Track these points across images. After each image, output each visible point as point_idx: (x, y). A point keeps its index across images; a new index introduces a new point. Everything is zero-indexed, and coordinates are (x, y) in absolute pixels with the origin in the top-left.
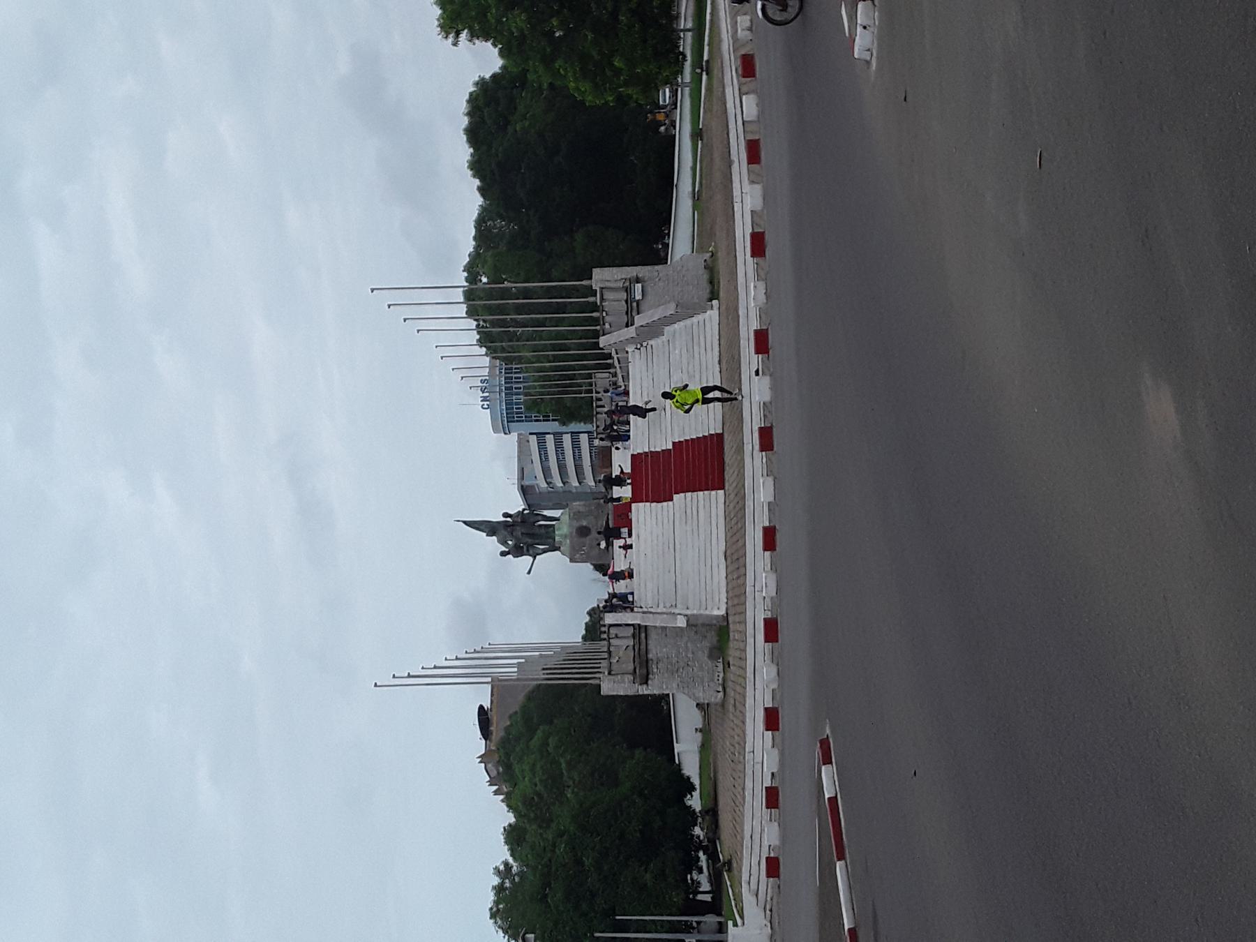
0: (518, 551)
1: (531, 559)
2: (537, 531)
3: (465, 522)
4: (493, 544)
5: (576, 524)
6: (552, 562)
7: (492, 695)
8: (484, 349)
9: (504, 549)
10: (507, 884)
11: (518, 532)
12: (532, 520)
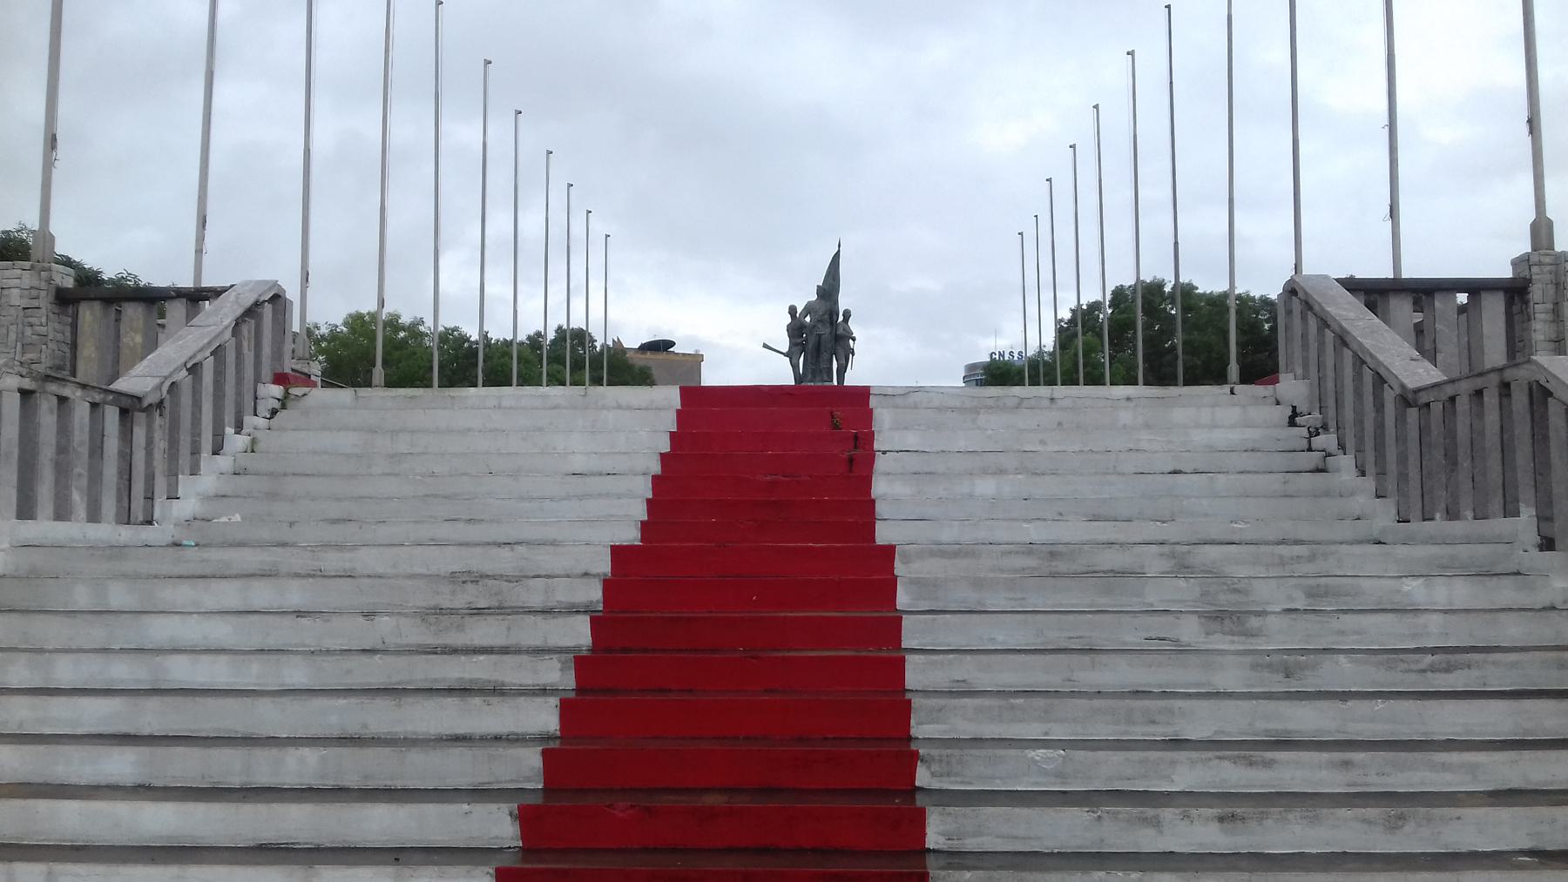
1: (785, 349)
2: (825, 356)
3: (837, 256)
4: (805, 296)
8: (1067, 315)
9: (799, 311)
10: (402, 334)
11: (825, 331)
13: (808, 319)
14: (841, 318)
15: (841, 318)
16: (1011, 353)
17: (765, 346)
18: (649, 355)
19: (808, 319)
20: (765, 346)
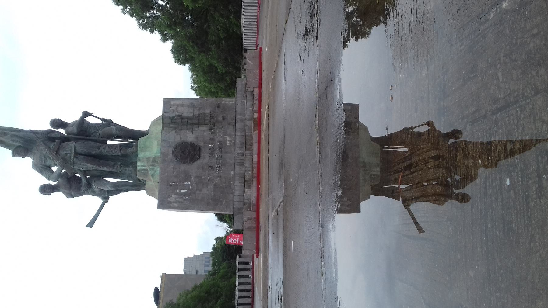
1: (98, 201)
2: (103, 151)
4: (24, 172)
5: (175, 138)
6: (135, 206)
7: (162, 283)
13: (55, 169)
15: (62, 131)
18: (161, 301)
19: (55, 169)
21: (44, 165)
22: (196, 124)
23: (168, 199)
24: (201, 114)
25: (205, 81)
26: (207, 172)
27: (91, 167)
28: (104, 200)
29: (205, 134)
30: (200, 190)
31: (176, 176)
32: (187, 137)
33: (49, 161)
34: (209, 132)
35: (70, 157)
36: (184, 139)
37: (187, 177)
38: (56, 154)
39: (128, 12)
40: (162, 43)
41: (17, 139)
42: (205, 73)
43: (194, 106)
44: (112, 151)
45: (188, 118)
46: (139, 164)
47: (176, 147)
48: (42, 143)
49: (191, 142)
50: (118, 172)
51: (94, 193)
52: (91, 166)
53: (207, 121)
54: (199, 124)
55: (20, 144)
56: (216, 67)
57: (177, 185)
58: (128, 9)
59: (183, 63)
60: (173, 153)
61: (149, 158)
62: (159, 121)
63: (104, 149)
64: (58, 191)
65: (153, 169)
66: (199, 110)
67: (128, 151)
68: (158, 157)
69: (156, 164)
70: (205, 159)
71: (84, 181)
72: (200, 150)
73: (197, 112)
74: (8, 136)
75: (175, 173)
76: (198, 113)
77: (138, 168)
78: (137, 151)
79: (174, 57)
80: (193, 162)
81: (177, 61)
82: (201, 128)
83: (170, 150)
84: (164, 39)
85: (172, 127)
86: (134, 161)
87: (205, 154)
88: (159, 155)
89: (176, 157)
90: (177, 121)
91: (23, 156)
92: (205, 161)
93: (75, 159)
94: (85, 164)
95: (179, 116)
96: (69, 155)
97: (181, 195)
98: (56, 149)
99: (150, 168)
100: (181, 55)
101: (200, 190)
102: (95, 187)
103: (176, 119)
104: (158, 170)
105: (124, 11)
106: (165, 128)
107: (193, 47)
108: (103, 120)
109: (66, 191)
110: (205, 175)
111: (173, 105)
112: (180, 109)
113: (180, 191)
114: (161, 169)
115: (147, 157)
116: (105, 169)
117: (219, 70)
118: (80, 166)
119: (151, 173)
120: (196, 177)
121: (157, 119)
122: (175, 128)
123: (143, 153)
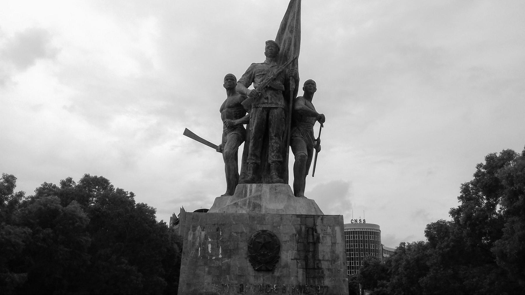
0: (234, 113)
1: (218, 142)
2: (274, 143)
5: (286, 234)
12: (299, 137)
14: (301, 93)
15: (301, 93)
16: (360, 220)
17: (188, 133)
19: (252, 87)
20: (188, 133)
21: (254, 74)
22: (307, 264)
23: (199, 227)
24: (323, 272)
25: (408, 262)
26: (236, 282)
27: (253, 128)
28: (219, 148)
29: (292, 278)
30: (209, 273)
31: (231, 236)
32: (287, 252)
33: (259, 80)
34: (295, 283)
35: (264, 103)
36: (284, 247)
37: (228, 253)
38: (267, 87)
39: (479, 171)
40: (449, 210)
41: (286, 45)
42: (417, 260)
43: (335, 261)
44: (273, 152)
45: (315, 252)
46: (254, 186)
47: (272, 236)
48: (281, 70)
49: (279, 257)
50: (247, 161)
51: (225, 135)
52: (254, 128)
53: (311, 281)
54: (307, 268)
55: (281, 49)
56: (425, 275)
57: (218, 239)
58: (483, 170)
59: (428, 234)
60: (263, 231)
61: (261, 198)
62: (313, 210)
63: (276, 143)
64: (229, 95)
65: (245, 205)
66: (329, 269)
67: (273, 171)
68: (260, 211)
69: (251, 208)
70: (255, 279)
71: (237, 121)
72: (268, 271)
73: (325, 265)
74: (289, 35)
75: (235, 234)
76: (323, 267)
77: (249, 185)
78: (273, 183)
79: (433, 224)
80: (250, 261)
81: (429, 227)
82: (301, 271)
83: (267, 227)
84: (453, 213)
85: (301, 229)
86: (263, 179)
87: (262, 279)
88: (263, 212)
89: (258, 235)
90: (311, 237)
91: (266, 54)
92: (252, 280)
93: (261, 109)
94: (256, 121)
95: (318, 238)
96: (266, 101)
97: (204, 245)
98: (272, 86)
99: (246, 201)
100: (436, 231)
101: (209, 273)
102: (231, 136)
103: (313, 235)
104: (244, 211)
105: (480, 166)
106: (299, 219)
107: (447, 246)
108: (318, 140)
109: (227, 103)
110: (230, 279)
111: (333, 230)
112: (328, 240)
113: (209, 242)
114: (242, 215)
115: (262, 196)
116: (251, 145)
117: (421, 280)
118: (253, 116)
119: (240, 201)
120: (229, 266)
121: (317, 208)
122: (299, 232)
123: (268, 190)
